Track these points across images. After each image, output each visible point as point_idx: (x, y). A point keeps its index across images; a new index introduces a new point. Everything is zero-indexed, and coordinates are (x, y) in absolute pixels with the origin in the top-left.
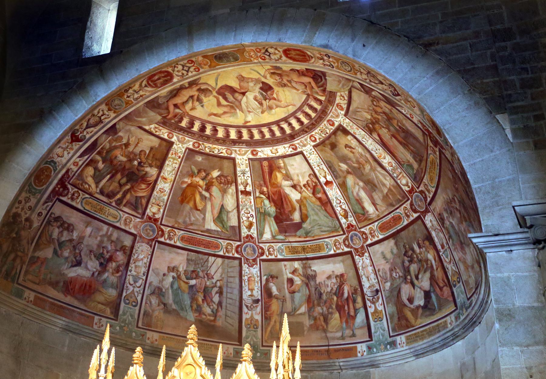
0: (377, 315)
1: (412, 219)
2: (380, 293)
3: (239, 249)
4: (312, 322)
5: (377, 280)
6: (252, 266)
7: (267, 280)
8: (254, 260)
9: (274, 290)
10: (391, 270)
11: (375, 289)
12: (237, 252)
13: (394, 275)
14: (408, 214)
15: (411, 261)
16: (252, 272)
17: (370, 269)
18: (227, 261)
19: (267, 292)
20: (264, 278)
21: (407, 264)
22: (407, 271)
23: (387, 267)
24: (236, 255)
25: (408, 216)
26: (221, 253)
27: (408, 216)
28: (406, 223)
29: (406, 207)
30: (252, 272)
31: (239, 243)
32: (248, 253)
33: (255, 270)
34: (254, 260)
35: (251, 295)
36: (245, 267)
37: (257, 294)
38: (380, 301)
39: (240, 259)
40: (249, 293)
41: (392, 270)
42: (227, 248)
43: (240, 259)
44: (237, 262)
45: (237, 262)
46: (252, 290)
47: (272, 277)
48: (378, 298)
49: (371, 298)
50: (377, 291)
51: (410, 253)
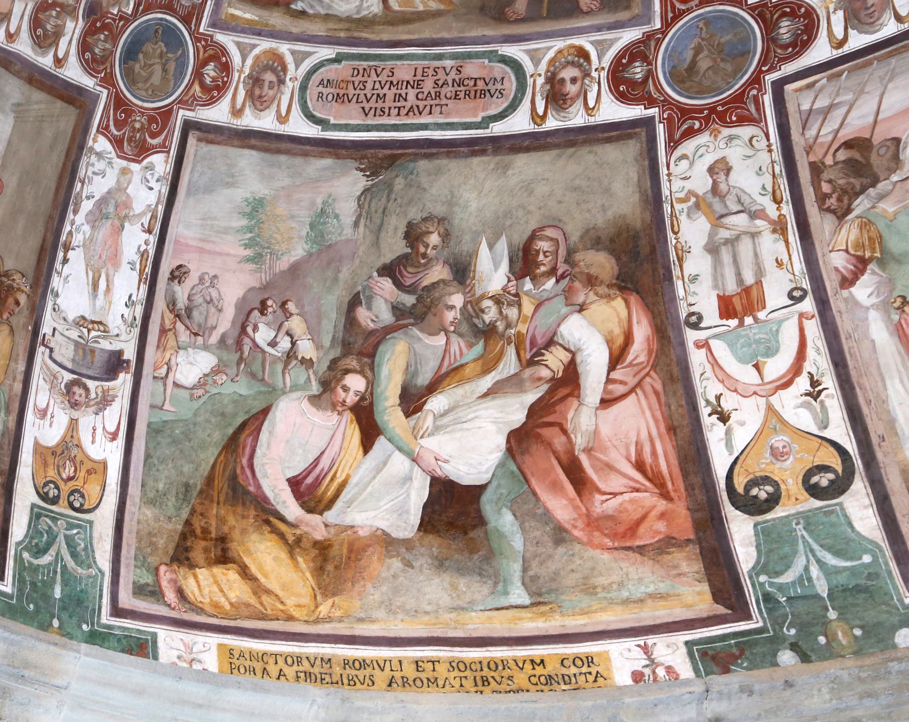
0: (69, 471)
1: (577, 118)
2: (124, 380)
5: (139, 311)
11: (106, 345)
14: (571, 89)
15: (419, 312)
17: (135, 240)
25: (557, 97)
27: (557, 97)
28: (519, 123)
29: (586, 56)
38: (115, 415)
41: (263, 308)
48: (105, 401)
49: (68, 377)
50: (114, 364)
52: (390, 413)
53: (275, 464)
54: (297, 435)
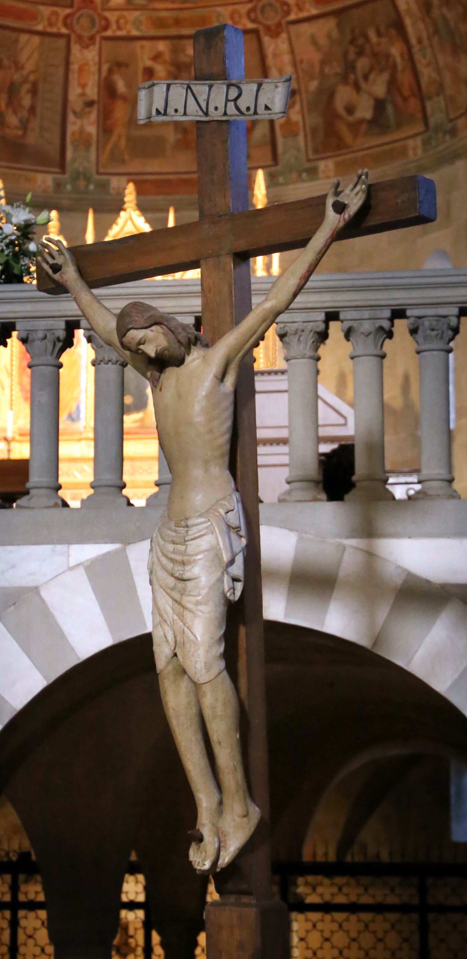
3: (69, 21)
4: (180, 136)
6: (87, 47)
7: (110, 71)
8: (92, 38)
9: (121, 86)
10: (323, 63)
12: (65, 25)
13: (327, 70)
16: (86, 57)
17: (287, 58)
18: (47, 40)
19: (108, 90)
20: (105, 67)
21: (352, 56)
22: (350, 67)
23: (317, 57)
24: (64, 31)
26: (40, 28)
30: (86, 57)
31: (68, 11)
32: (83, 27)
33: (91, 54)
34: (92, 38)
35: (83, 95)
36: (75, 49)
37: (92, 92)
39: (68, 37)
40: (79, 91)
42: (49, 19)
43: (68, 37)
44: (62, 42)
45: (62, 42)
46: (83, 86)
47: (119, 65)
51: (360, 41)
52: (363, 84)
53: (339, 105)
54: (344, 95)
